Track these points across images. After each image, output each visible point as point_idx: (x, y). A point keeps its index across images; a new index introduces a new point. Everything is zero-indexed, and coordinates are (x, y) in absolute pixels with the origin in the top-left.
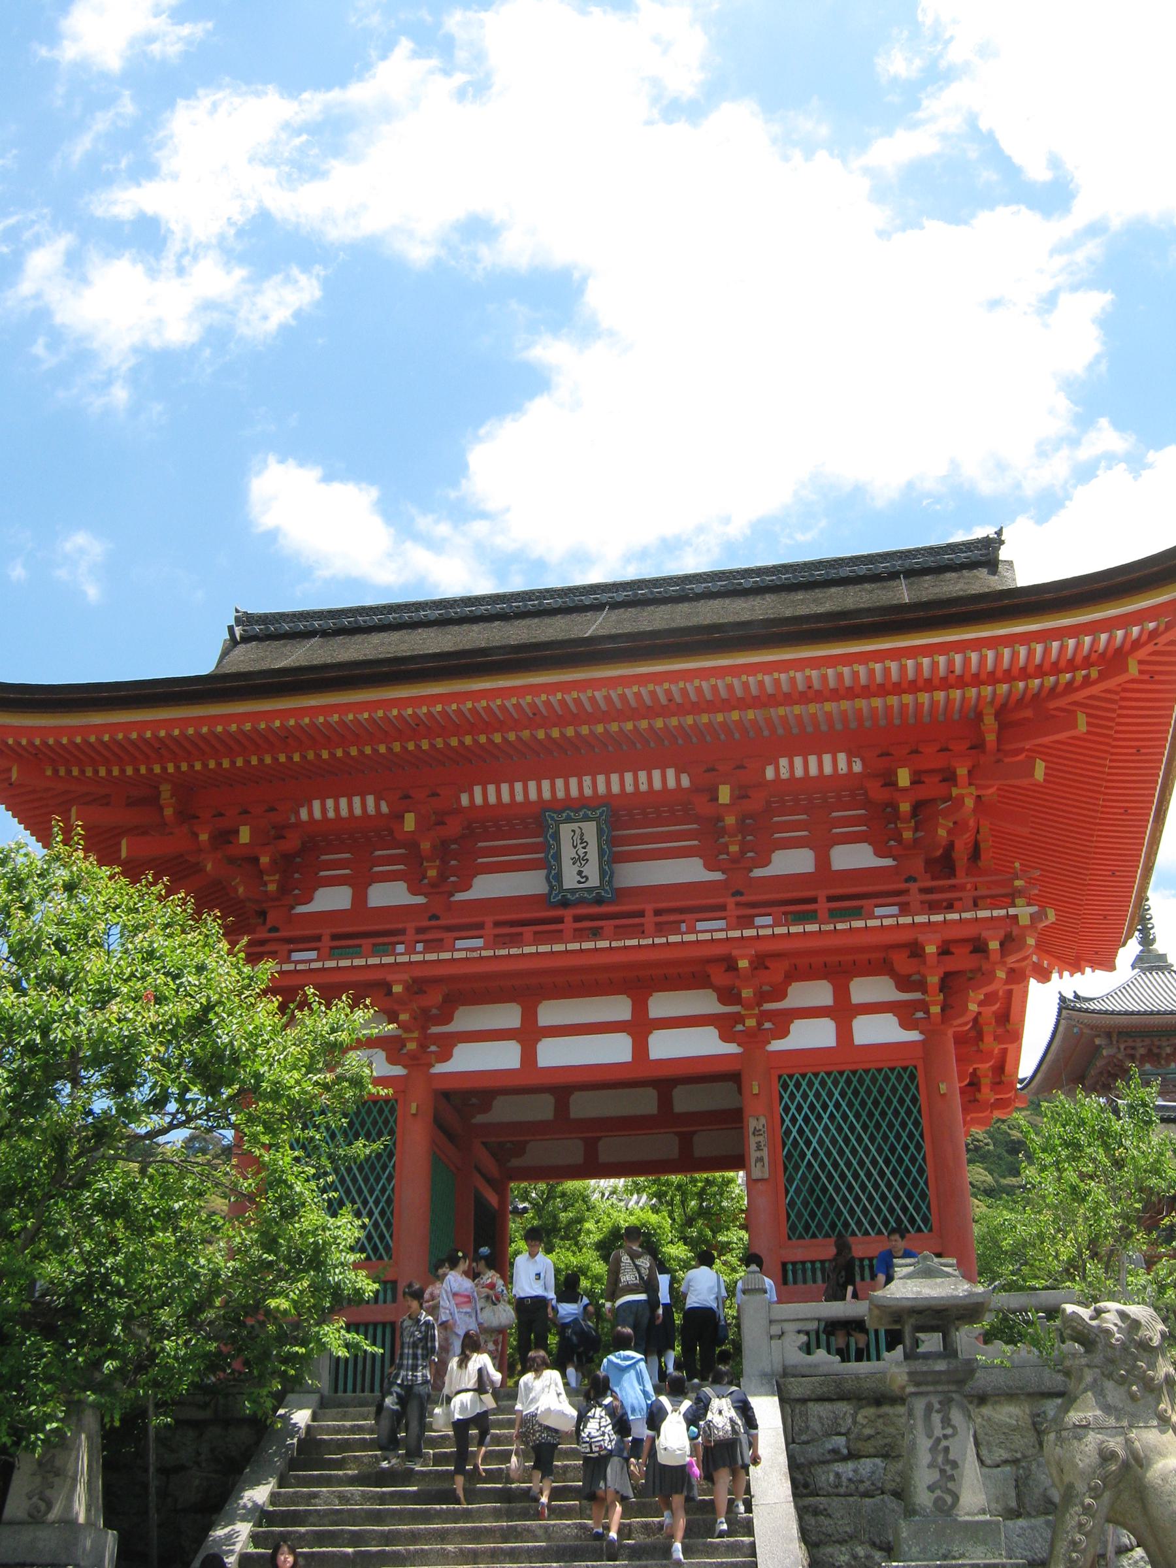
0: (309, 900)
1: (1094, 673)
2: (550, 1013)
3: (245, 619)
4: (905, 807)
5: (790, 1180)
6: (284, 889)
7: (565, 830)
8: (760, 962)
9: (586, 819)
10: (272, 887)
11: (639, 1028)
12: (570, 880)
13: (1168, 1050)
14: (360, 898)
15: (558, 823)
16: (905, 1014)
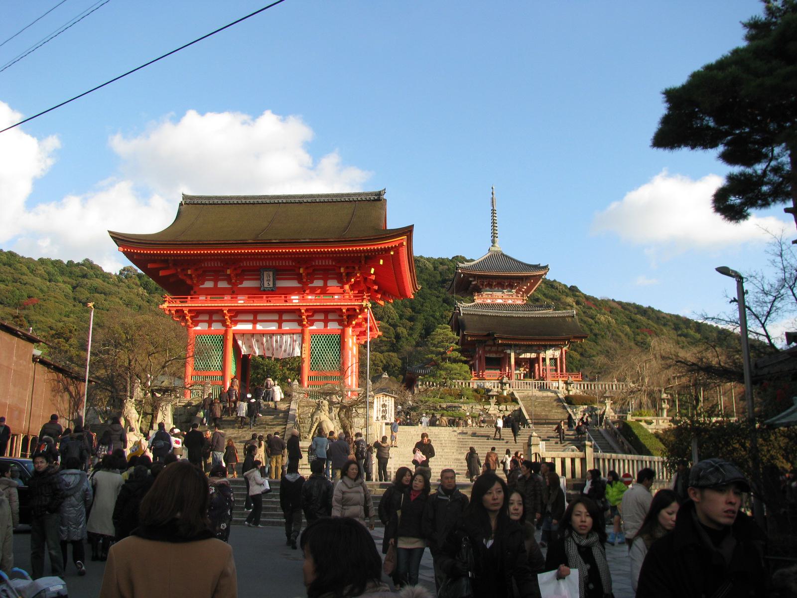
0: (203, 284)
1: (384, 253)
2: (259, 317)
3: (185, 197)
4: (344, 274)
5: (311, 358)
6: (198, 281)
7: (265, 273)
8: (307, 310)
9: (270, 271)
10: (195, 282)
11: (280, 322)
12: (266, 285)
13: (494, 283)
14: (216, 284)
15: (264, 271)
16: (340, 322)
